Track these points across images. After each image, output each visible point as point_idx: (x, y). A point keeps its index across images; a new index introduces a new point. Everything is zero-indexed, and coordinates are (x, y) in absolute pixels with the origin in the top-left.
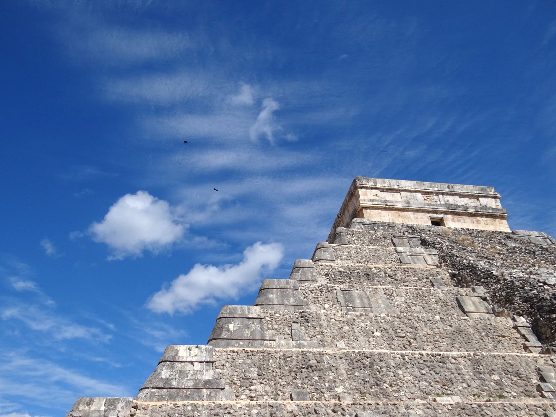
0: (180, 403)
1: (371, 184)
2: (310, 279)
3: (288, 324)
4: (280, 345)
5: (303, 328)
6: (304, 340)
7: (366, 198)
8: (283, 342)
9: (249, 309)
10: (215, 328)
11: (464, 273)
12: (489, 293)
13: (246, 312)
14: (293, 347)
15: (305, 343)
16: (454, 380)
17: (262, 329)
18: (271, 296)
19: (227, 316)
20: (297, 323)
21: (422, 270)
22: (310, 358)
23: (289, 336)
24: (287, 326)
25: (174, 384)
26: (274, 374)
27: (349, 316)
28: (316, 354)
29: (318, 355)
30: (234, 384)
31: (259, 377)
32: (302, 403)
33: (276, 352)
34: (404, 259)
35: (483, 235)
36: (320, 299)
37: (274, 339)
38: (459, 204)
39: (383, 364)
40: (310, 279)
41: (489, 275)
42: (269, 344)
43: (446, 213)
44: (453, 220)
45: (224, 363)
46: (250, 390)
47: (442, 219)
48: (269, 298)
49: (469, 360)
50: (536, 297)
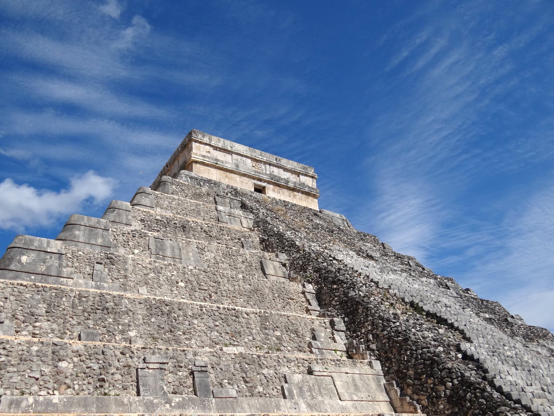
1: (206, 140)
2: (124, 222)
3: (90, 263)
4: (77, 283)
5: (106, 270)
6: (105, 282)
7: (198, 152)
8: (81, 281)
9: (48, 243)
10: (3, 258)
11: (272, 239)
12: (289, 260)
13: (45, 245)
14: (92, 287)
15: (106, 285)
16: (242, 333)
17: (60, 265)
18: (77, 233)
19: (21, 246)
20: (101, 264)
21: (237, 231)
22: (108, 300)
23: (89, 276)
24: (89, 265)
26: (65, 312)
27: (157, 264)
28: (114, 297)
29: (117, 299)
30: (16, 319)
31: (47, 314)
32: (90, 344)
33: (72, 291)
34: (222, 217)
35: (296, 209)
36: (130, 243)
37: (72, 277)
38: (282, 177)
39: (181, 313)
40: (124, 222)
41: (292, 244)
42: (65, 282)
43: (269, 182)
44: (274, 190)
45: (8, 296)
46: (34, 327)
47: (264, 187)
48: (76, 235)
49: (259, 316)
50: (325, 269)
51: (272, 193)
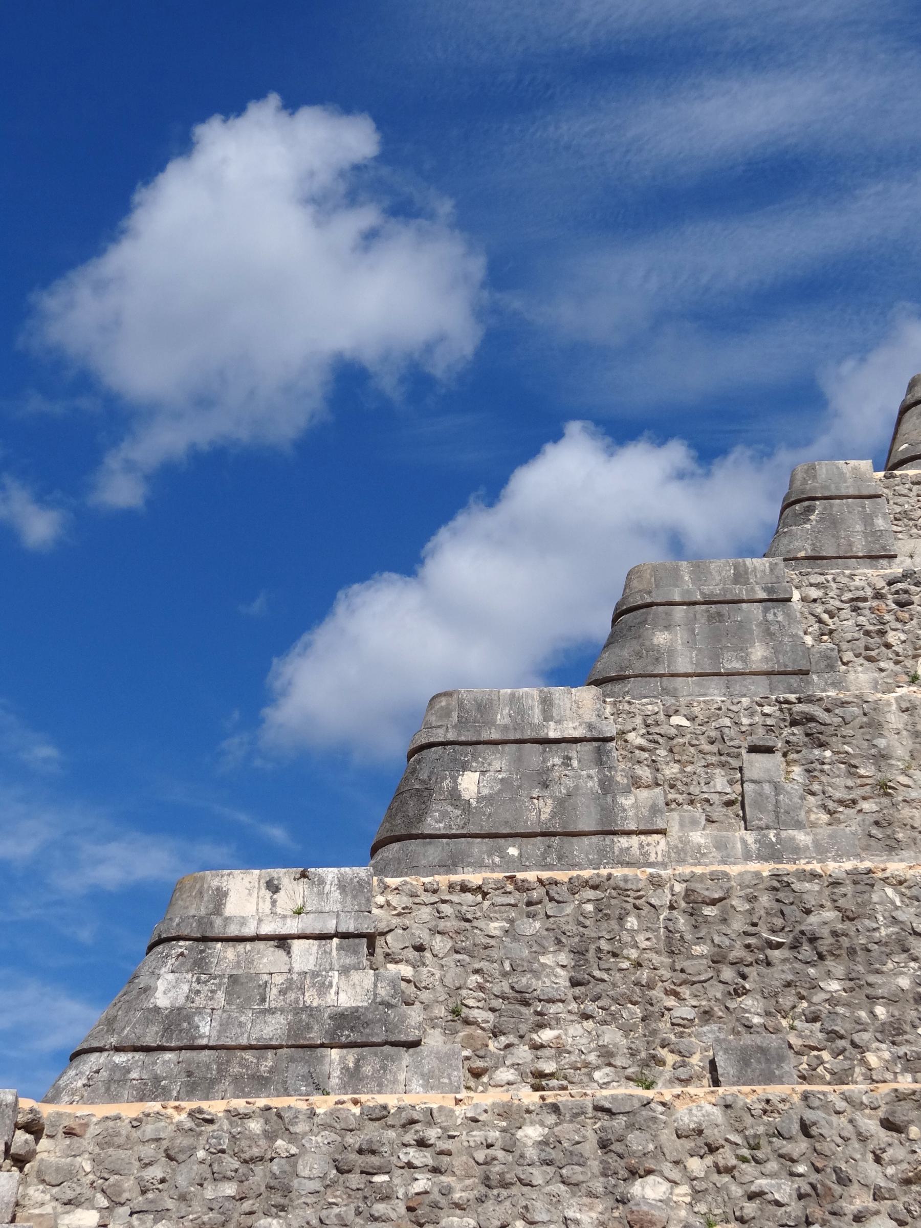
0: (215, 1107)
2: (860, 548)
3: (725, 756)
4: (690, 849)
5: (797, 770)
6: (799, 825)
8: (698, 837)
9: (547, 703)
10: (399, 793)
13: (536, 716)
14: (748, 857)
15: (802, 838)
17: (607, 786)
18: (661, 638)
19: (451, 736)
20: (769, 750)
22: (811, 902)
23: (730, 811)
24: (723, 765)
25: (206, 1029)
26: (644, 975)
28: (836, 884)
29: (849, 889)
30: (467, 1022)
31: (578, 991)
32: (749, 1095)
33: (656, 883)
36: (892, 637)
37: (660, 825)
40: (860, 548)
42: (635, 850)
45: (424, 936)
46: (537, 1047)
48: (652, 648)
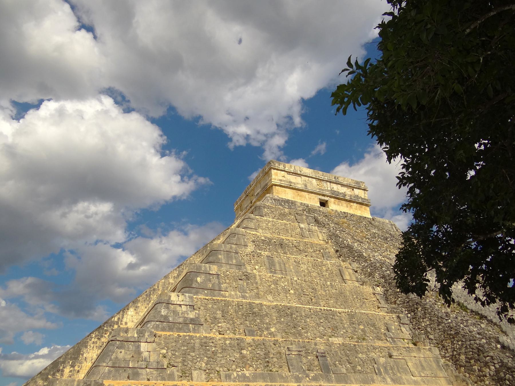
0: (181, 334)
1: (281, 167)
6: (246, 293)
7: (276, 178)
9: (210, 267)
11: (345, 250)
13: (208, 269)
16: (338, 327)
17: (219, 282)
18: (220, 256)
21: (317, 244)
25: (171, 319)
27: (274, 278)
34: (304, 233)
35: (355, 219)
36: (252, 261)
38: (340, 192)
39: (298, 314)
40: (243, 244)
41: (361, 256)
43: (331, 197)
44: (335, 203)
47: (327, 201)
48: (219, 258)
49: (348, 314)
50: (389, 276)
51: (334, 206)
